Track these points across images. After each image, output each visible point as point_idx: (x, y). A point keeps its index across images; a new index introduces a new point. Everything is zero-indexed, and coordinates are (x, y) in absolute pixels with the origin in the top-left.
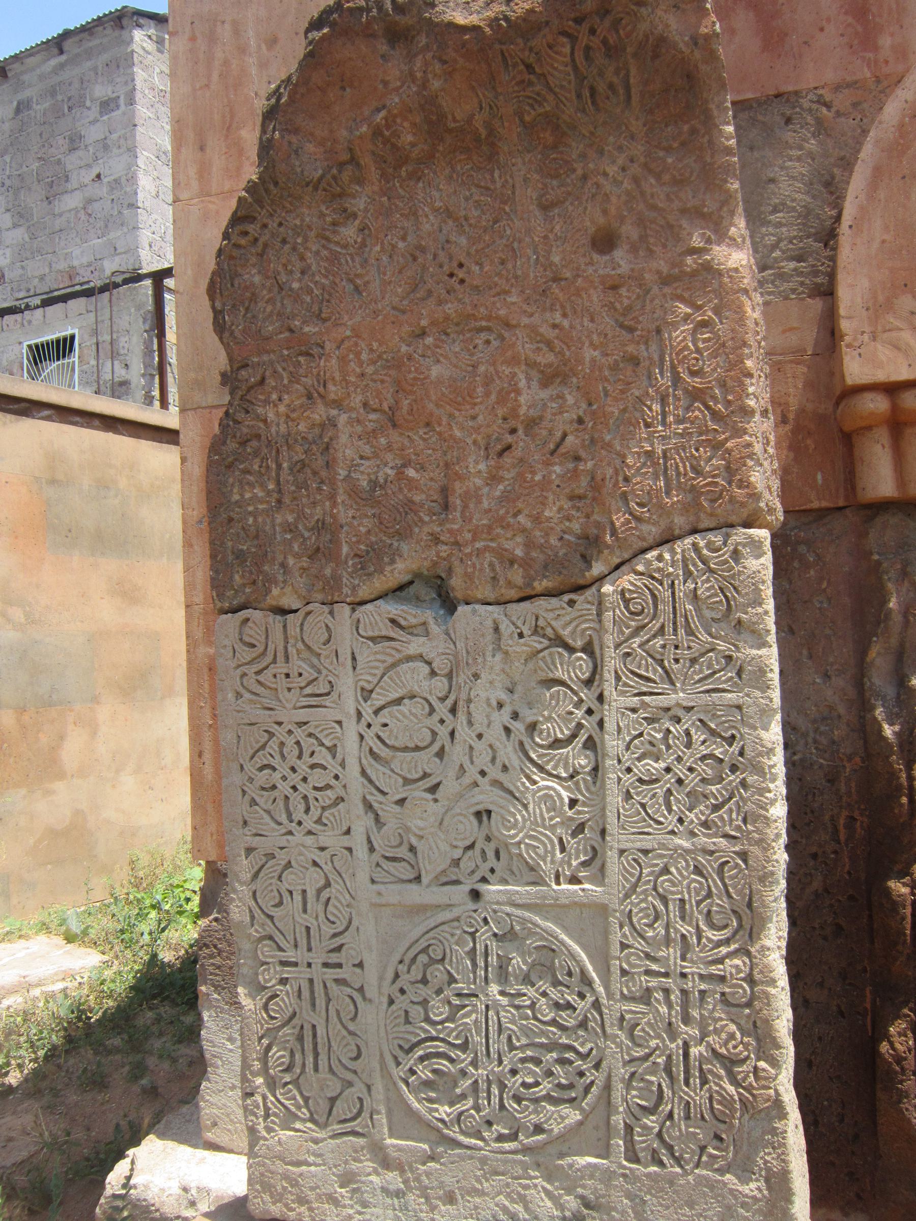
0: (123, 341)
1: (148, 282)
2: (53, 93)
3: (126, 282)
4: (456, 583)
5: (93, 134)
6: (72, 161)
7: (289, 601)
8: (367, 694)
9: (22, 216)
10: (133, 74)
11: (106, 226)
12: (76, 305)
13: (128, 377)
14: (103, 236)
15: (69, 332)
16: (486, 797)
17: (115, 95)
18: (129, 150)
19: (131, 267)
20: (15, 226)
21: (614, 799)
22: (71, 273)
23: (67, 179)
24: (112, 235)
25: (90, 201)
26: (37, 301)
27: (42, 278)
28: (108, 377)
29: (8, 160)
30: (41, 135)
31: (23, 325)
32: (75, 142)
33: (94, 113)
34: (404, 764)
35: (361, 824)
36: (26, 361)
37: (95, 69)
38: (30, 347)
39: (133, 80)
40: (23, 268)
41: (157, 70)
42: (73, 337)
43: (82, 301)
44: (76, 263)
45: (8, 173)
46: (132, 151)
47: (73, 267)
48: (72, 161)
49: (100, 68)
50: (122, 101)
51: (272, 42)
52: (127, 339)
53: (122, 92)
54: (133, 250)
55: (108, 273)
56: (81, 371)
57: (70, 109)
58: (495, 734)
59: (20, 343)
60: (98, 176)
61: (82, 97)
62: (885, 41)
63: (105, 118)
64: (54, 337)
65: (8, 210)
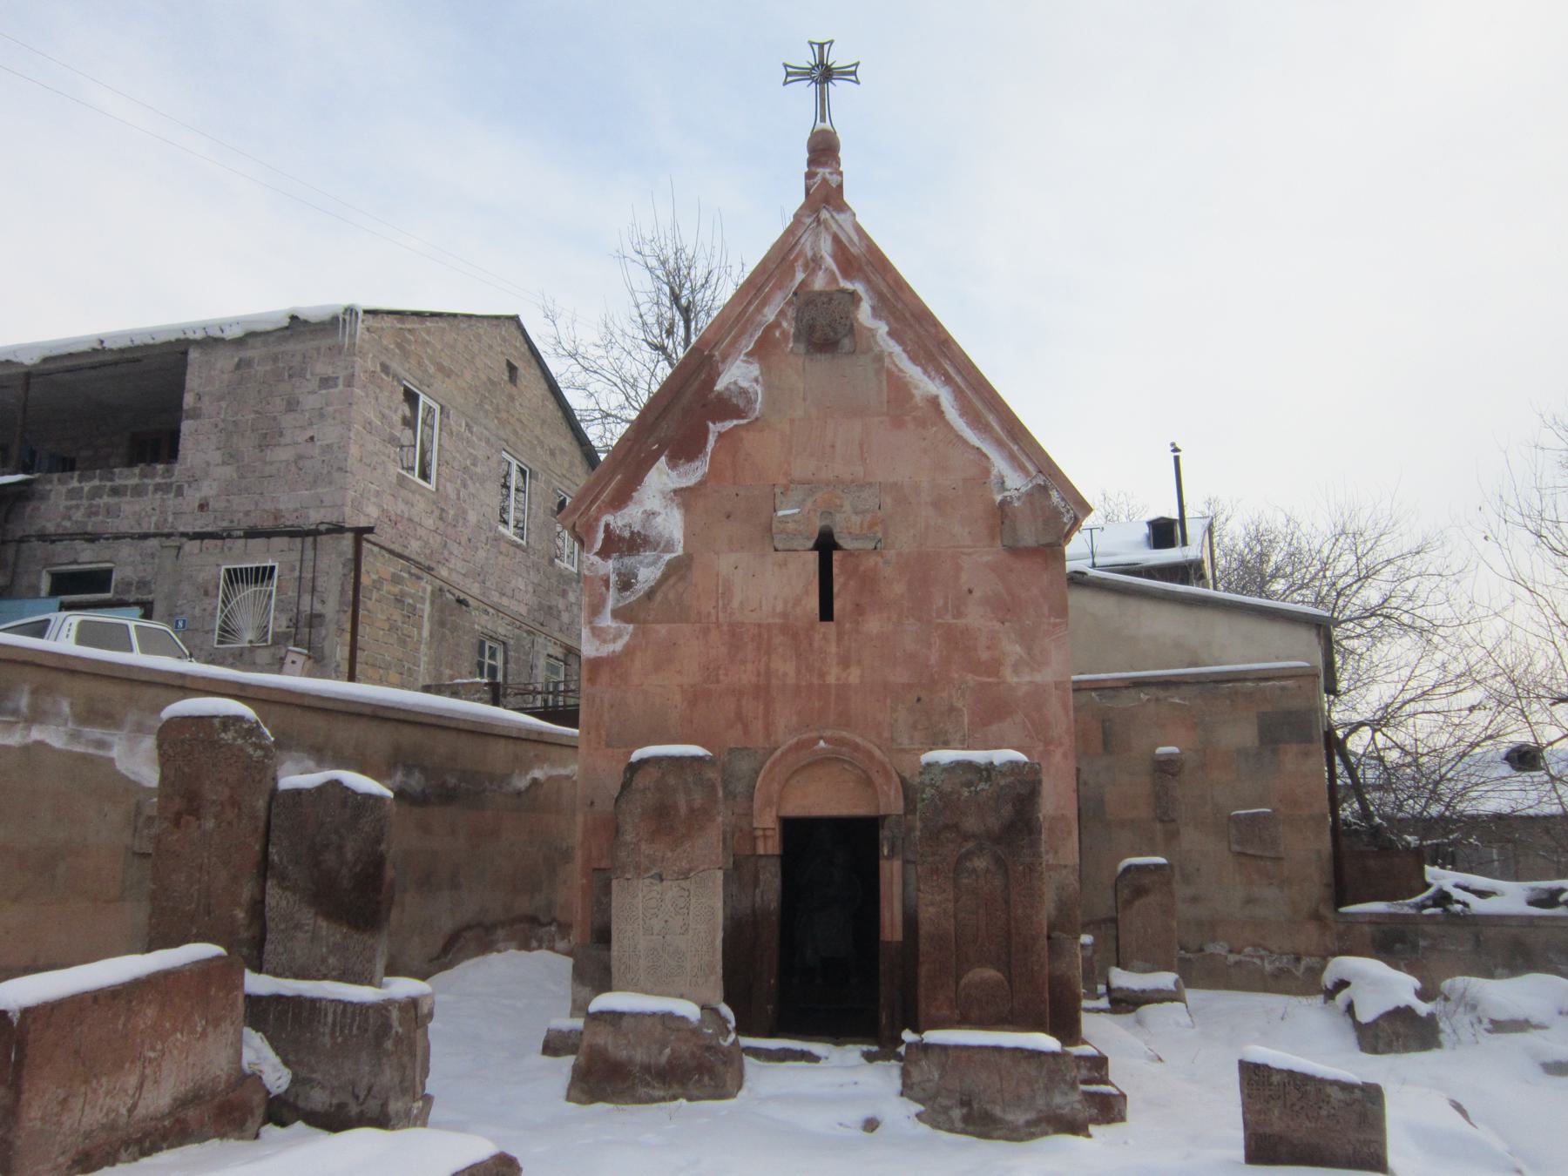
0: (320, 581)
1: (349, 536)
2: (275, 360)
3: (328, 532)
4: (664, 876)
5: (310, 402)
6: (287, 421)
7: (628, 876)
8: (644, 897)
9: (231, 456)
10: (354, 362)
11: (315, 482)
13: (323, 611)
14: (311, 489)
15: (269, 563)
16: (667, 918)
17: (335, 375)
18: (343, 422)
19: (334, 520)
20: (224, 463)
21: (691, 918)
22: (277, 515)
23: (281, 434)
24: (320, 490)
25: (300, 457)
27: (247, 513)
28: (308, 609)
29: (224, 406)
30: (259, 392)
31: (223, 549)
32: (292, 405)
33: (314, 384)
34: (652, 911)
35: (641, 923)
36: (222, 582)
37: (318, 349)
38: (228, 571)
39: (353, 367)
40: (228, 501)
41: (371, 355)
42: (273, 568)
43: (286, 540)
44: (282, 506)
45: (222, 416)
47: (279, 511)
48: (287, 421)
49: (323, 350)
50: (341, 382)
51: (612, 706)
52: (326, 578)
53: (342, 374)
55: (312, 520)
56: (279, 601)
57: (290, 376)
58: (669, 906)
59: (218, 565)
60: (312, 438)
61: (304, 369)
62: (772, 738)
63: (324, 392)
64: (254, 565)
65: (218, 449)
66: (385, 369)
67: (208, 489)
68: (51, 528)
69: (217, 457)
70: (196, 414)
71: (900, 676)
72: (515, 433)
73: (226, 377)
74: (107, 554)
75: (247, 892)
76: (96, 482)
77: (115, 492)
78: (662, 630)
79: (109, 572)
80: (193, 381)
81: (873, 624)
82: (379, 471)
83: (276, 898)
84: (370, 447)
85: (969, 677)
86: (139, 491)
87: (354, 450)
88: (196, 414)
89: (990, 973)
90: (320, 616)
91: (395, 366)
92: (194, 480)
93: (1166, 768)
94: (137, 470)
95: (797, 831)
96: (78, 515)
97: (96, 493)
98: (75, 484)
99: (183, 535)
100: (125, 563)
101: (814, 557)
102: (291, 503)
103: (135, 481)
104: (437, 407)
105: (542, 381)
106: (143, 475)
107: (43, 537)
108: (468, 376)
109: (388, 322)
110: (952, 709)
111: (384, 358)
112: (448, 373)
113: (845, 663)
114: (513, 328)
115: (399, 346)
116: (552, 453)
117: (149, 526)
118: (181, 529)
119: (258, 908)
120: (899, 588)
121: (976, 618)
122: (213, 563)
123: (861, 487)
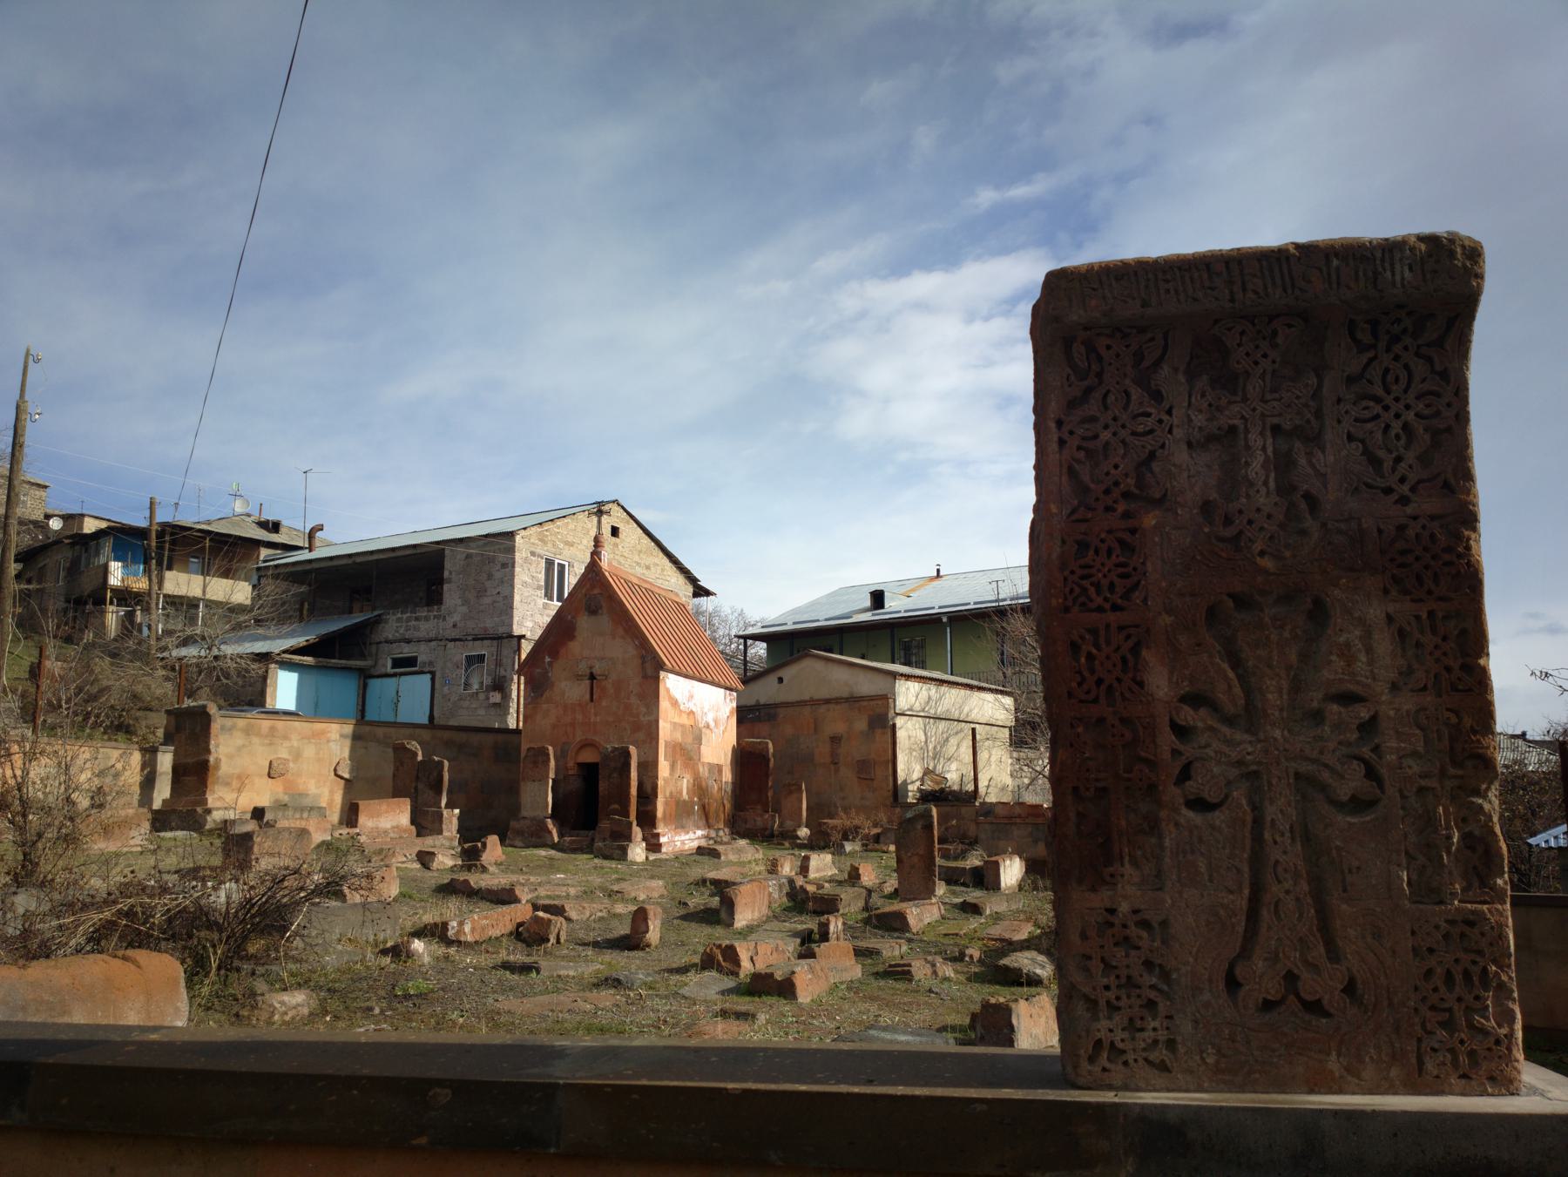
0: (504, 660)
1: (515, 641)
5: (498, 575)
6: (488, 584)
12: (487, 642)
20: (463, 605)
22: (486, 629)
25: (494, 602)
26: (470, 638)
32: (490, 577)
46: (512, 586)
54: (511, 625)
66: (533, 554)
67: (456, 618)
68: (390, 637)
69: (459, 602)
70: (450, 581)
71: (611, 719)
72: (620, 563)
73: (462, 563)
74: (415, 649)
75: (414, 785)
76: (409, 615)
77: (417, 619)
78: (545, 706)
79: (415, 659)
80: (448, 565)
81: (604, 704)
82: (532, 604)
83: (421, 786)
84: (526, 594)
85: (631, 719)
86: (427, 619)
87: (517, 598)
88: (450, 581)
89: (616, 806)
90: (505, 677)
91: (538, 551)
92: (450, 613)
93: (835, 740)
94: (426, 609)
95: (581, 765)
96: (402, 631)
97: (408, 620)
98: (399, 615)
99: (447, 639)
100: (423, 653)
101: (588, 682)
102: (490, 623)
103: (425, 614)
104: (567, 564)
105: (639, 529)
106: (428, 611)
107: (388, 642)
108: (585, 542)
109: (534, 529)
110: (625, 729)
111: (533, 549)
112: (571, 544)
113: (596, 715)
114: (615, 508)
115: (540, 540)
116: (648, 568)
117: (432, 635)
118: (447, 636)
119: (416, 789)
120: (612, 691)
121: (634, 700)
122: (459, 653)
123: (603, 659)
